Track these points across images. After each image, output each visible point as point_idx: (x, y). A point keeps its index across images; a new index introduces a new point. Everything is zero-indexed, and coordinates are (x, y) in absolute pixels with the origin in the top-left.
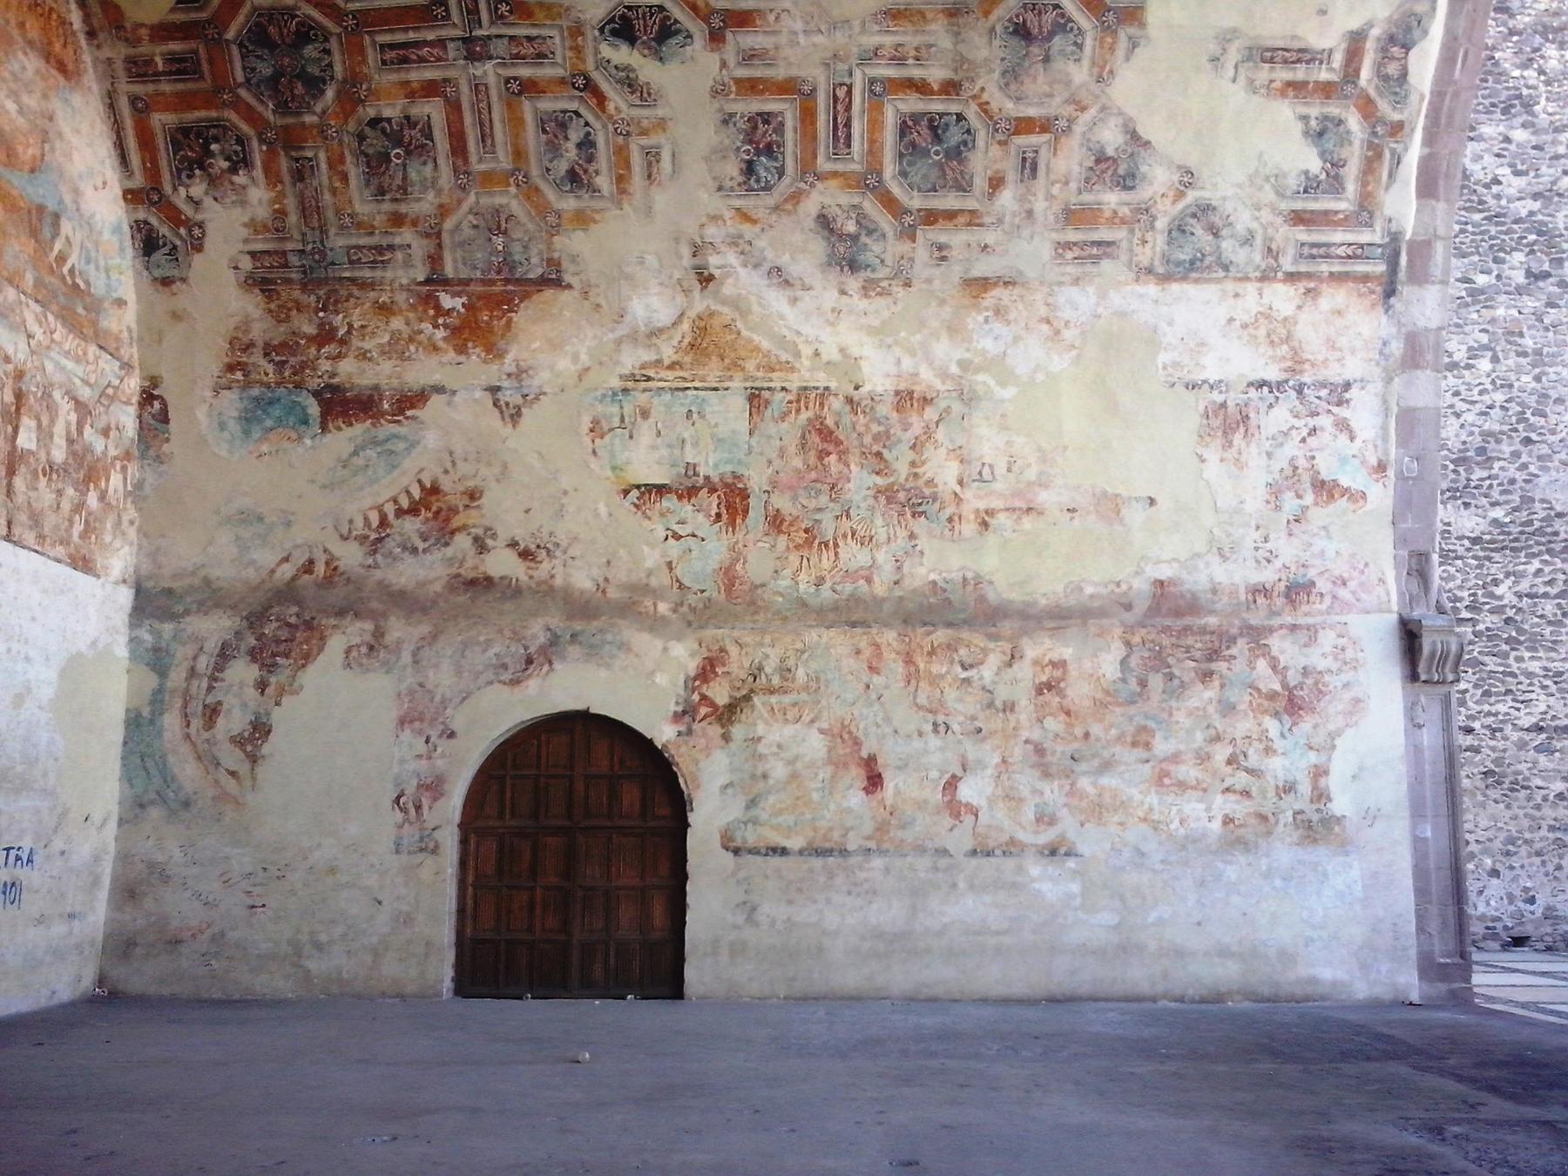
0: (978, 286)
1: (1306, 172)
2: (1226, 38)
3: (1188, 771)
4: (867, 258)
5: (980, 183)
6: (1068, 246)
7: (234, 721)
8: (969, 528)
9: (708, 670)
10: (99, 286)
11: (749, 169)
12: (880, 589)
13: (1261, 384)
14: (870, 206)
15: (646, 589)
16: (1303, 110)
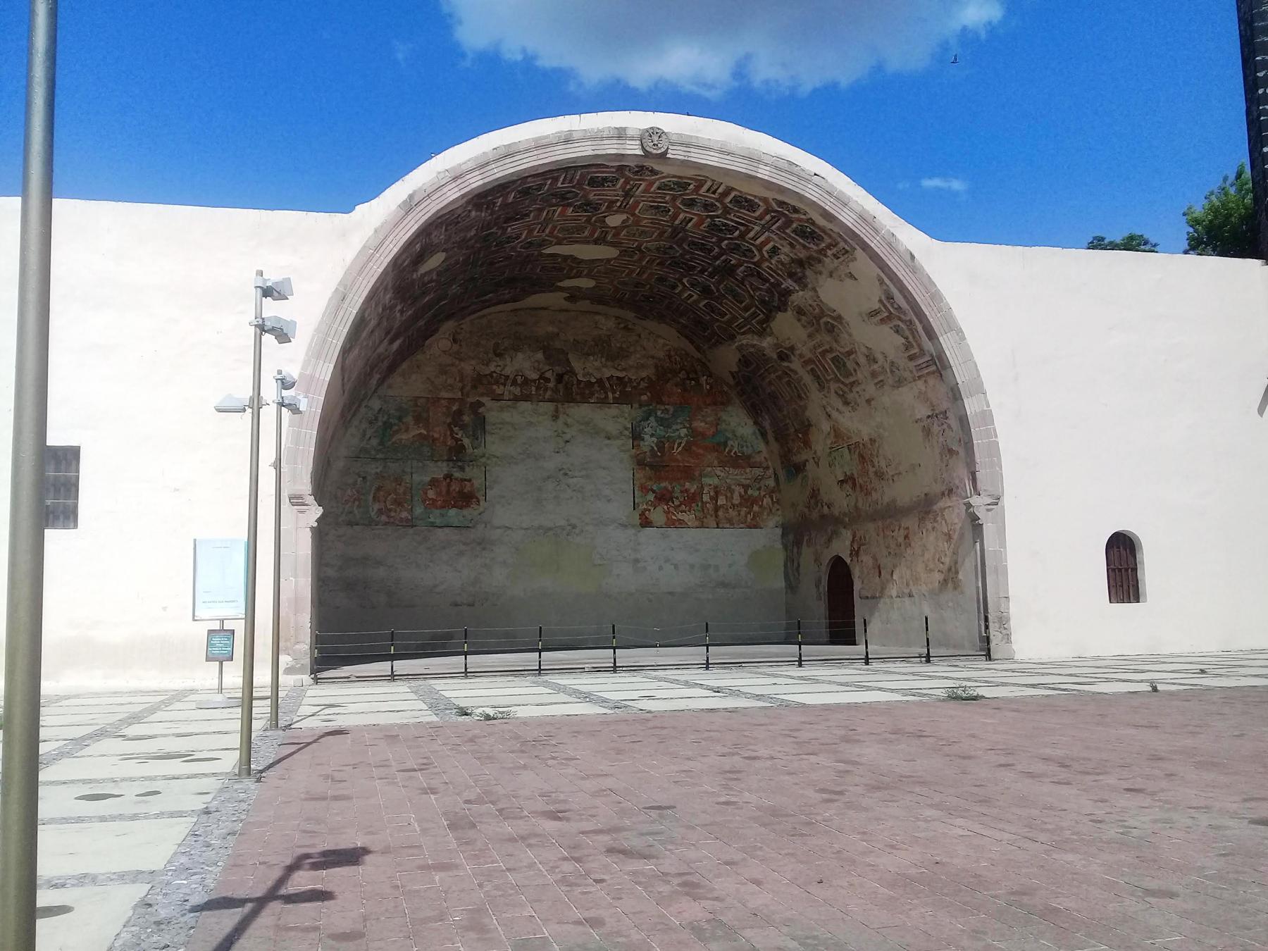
0: (869, 401)
1: (903, 344)
2: (860, 314)
3: (932, 566)
4: (849, 401)
5: (853, 372)
6: (876, 384)
7: (796, 564)
8: (891, 481)
9: (853, 541)
10: (748, 451)
11: (819, 384)
12: (879, 507)
13: (929, 417)
14: (842, 386)
15: (845, 514)
16: (890, 326)
